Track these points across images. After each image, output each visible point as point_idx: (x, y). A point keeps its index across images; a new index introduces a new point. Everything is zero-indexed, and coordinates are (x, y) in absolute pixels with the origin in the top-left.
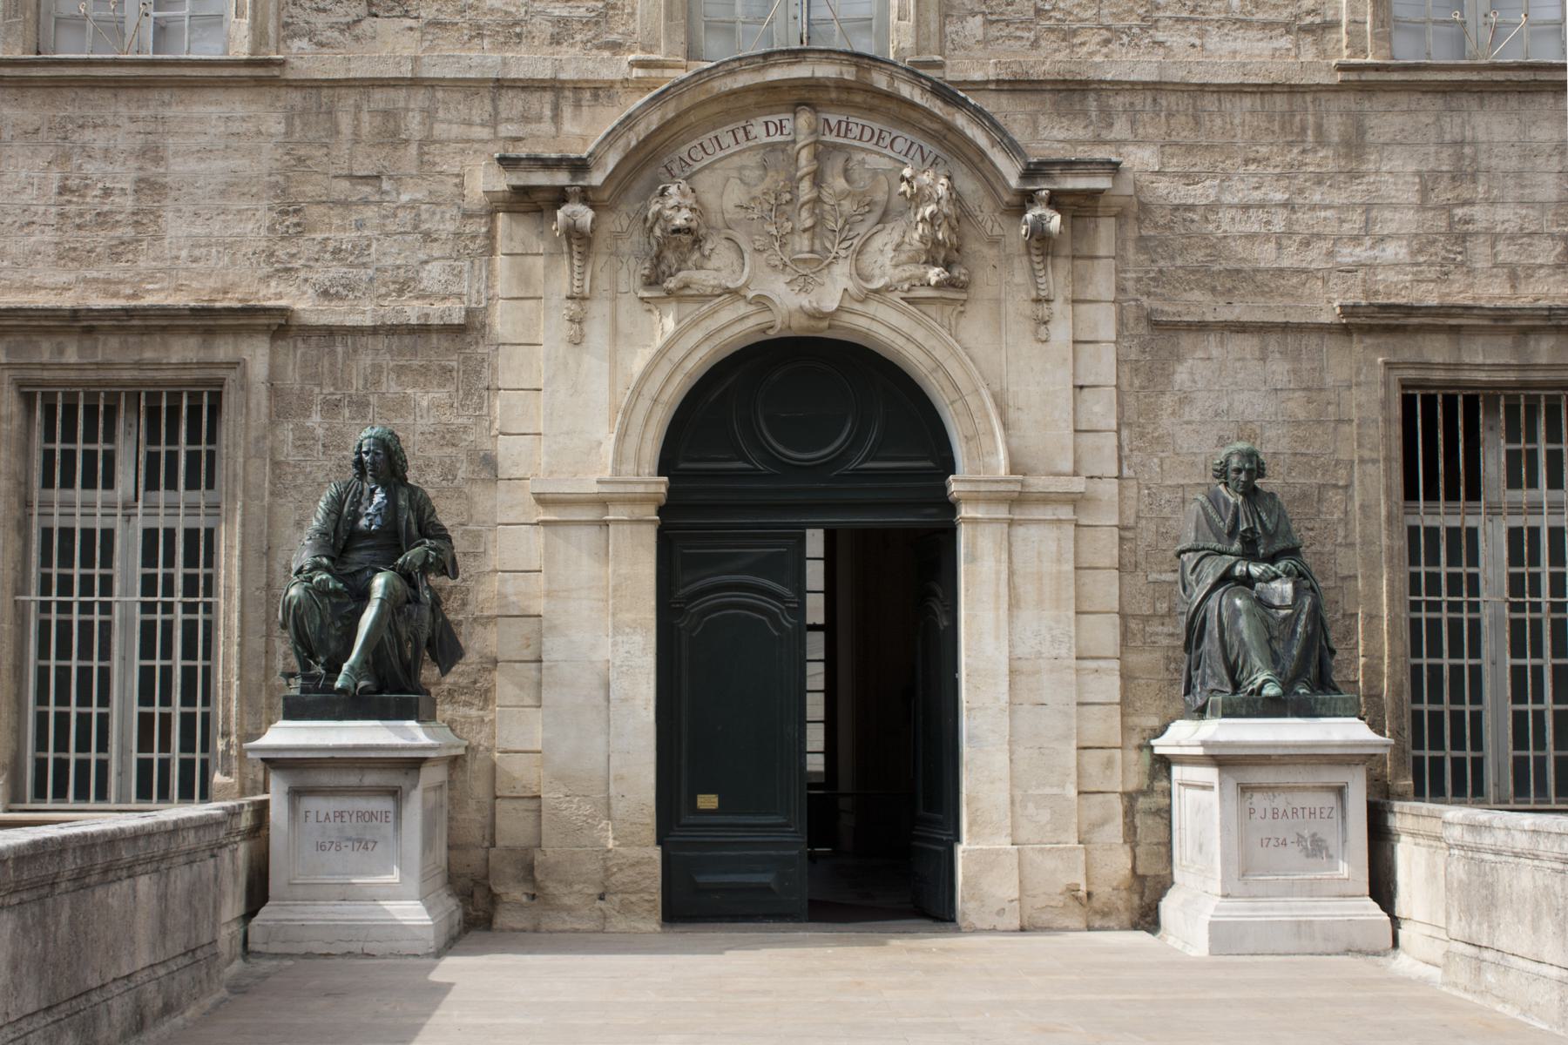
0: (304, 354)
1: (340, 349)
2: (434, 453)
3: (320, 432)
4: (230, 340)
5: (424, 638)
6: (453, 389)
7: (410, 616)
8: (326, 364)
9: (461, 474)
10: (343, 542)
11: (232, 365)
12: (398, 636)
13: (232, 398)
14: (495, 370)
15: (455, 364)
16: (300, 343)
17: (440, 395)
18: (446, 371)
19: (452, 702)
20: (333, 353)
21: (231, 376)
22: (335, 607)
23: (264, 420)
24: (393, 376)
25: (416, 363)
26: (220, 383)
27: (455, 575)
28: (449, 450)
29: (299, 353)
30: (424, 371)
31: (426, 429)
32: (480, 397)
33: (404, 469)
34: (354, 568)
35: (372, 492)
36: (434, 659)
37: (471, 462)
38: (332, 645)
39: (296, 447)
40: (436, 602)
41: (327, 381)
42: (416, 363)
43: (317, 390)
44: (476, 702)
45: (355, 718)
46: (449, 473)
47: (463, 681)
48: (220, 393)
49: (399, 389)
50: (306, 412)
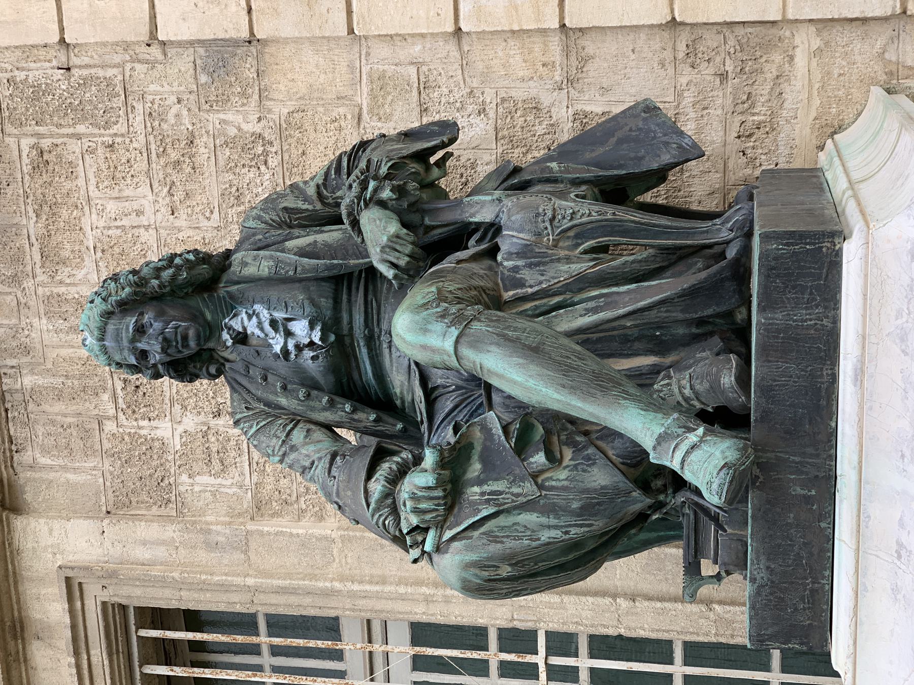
0: (45, 451)
1: (28, 381)
2: (211, 186)
3: (190, 422)
4: (27, 585)
5: (590, 211)
6: (75, 147)
7: (524, 252)
8: (59, 407)
9: (251, 127)
10: (360, 403)
11: (73, 589)
12: (582, 283)
13: (138, 592)
14: (27, 50)
15: (26, 143)
16: (26, 457)
17: (87, 179)
18: (42, 161)
19: (770, 126)
20: (35, 394)
21: (95, 597)
22: (491, 470)
23: (171, 531)
24: (64, 273)
25: (33, 226)
26: (117, 616)
27: (448, 132)
28: (203, 151)
29: (44, 461)
30: (47, 208)
31: (164, 201)
32: (86, 82)
33: (204, 258)
34: (419, 393)
35: (242, 338)
36: (659, 176)
37: (223, 101)
38: (601, 477)
39: (224, 468)
40: (513, 180)
41: (88, 407)
42: (33, 226)
43: (110, 426)
44: (771, 71)
45: (833, 435)
46: (251, 149)
47: (721, 99)
48: (140, 611)
49: (89, 263)
50: (154, 448)
